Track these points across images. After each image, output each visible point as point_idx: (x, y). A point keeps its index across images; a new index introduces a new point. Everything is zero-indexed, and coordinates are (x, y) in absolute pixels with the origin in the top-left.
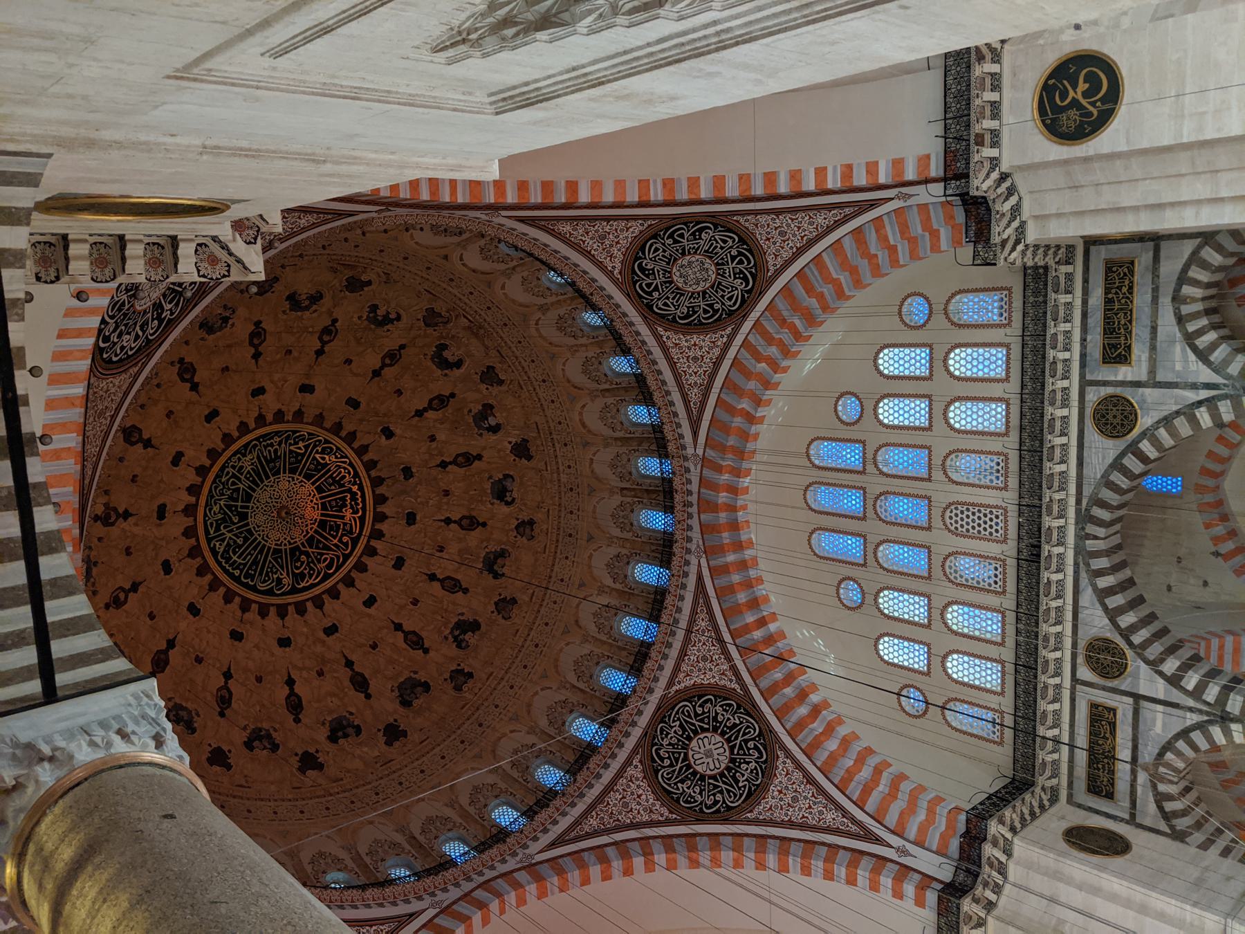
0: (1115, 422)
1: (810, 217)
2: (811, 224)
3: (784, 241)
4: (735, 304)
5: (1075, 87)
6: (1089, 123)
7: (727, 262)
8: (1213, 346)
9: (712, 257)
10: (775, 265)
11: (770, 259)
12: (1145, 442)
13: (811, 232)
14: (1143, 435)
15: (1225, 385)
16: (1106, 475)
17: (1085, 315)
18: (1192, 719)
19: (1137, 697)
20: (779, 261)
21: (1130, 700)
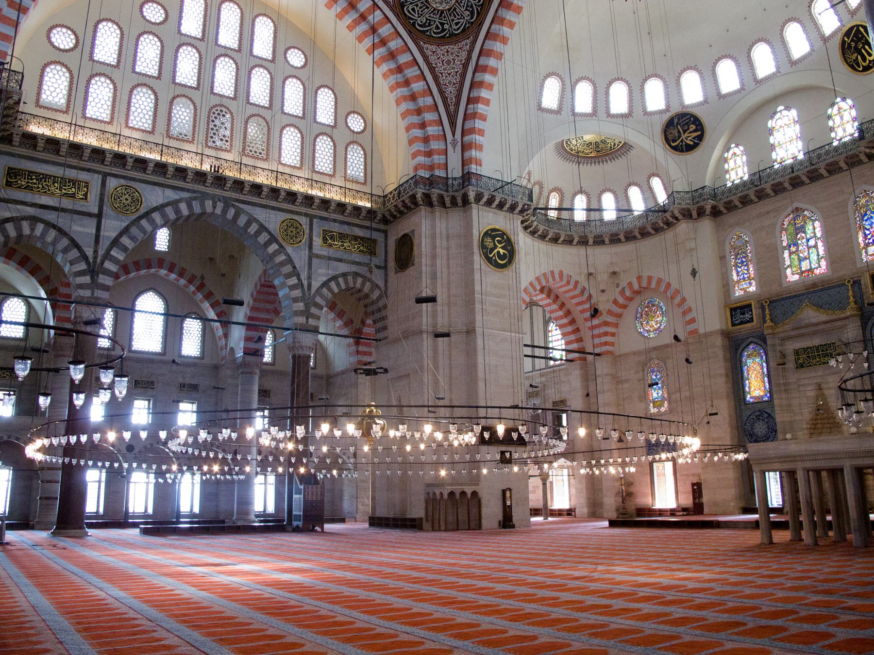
0: (294, 234)
1: (454, 84)
2: (450, 82)
3: (443, 61)
4: (409, 12)
5: (502, 248)
6: (487, 252)
7: (441, 19)
8: (330, 289)
9: (449, 11)
10: (427, 49)
11: (433, 48)
12: (277, 247)
13: (444, 80)
14: (281, 246)
15: (310, 294)
16: (257, 221)
17: (349, 224)
18: (89, 252)
19: (99, 216)
20: (429, 53)
21: (95, 210)
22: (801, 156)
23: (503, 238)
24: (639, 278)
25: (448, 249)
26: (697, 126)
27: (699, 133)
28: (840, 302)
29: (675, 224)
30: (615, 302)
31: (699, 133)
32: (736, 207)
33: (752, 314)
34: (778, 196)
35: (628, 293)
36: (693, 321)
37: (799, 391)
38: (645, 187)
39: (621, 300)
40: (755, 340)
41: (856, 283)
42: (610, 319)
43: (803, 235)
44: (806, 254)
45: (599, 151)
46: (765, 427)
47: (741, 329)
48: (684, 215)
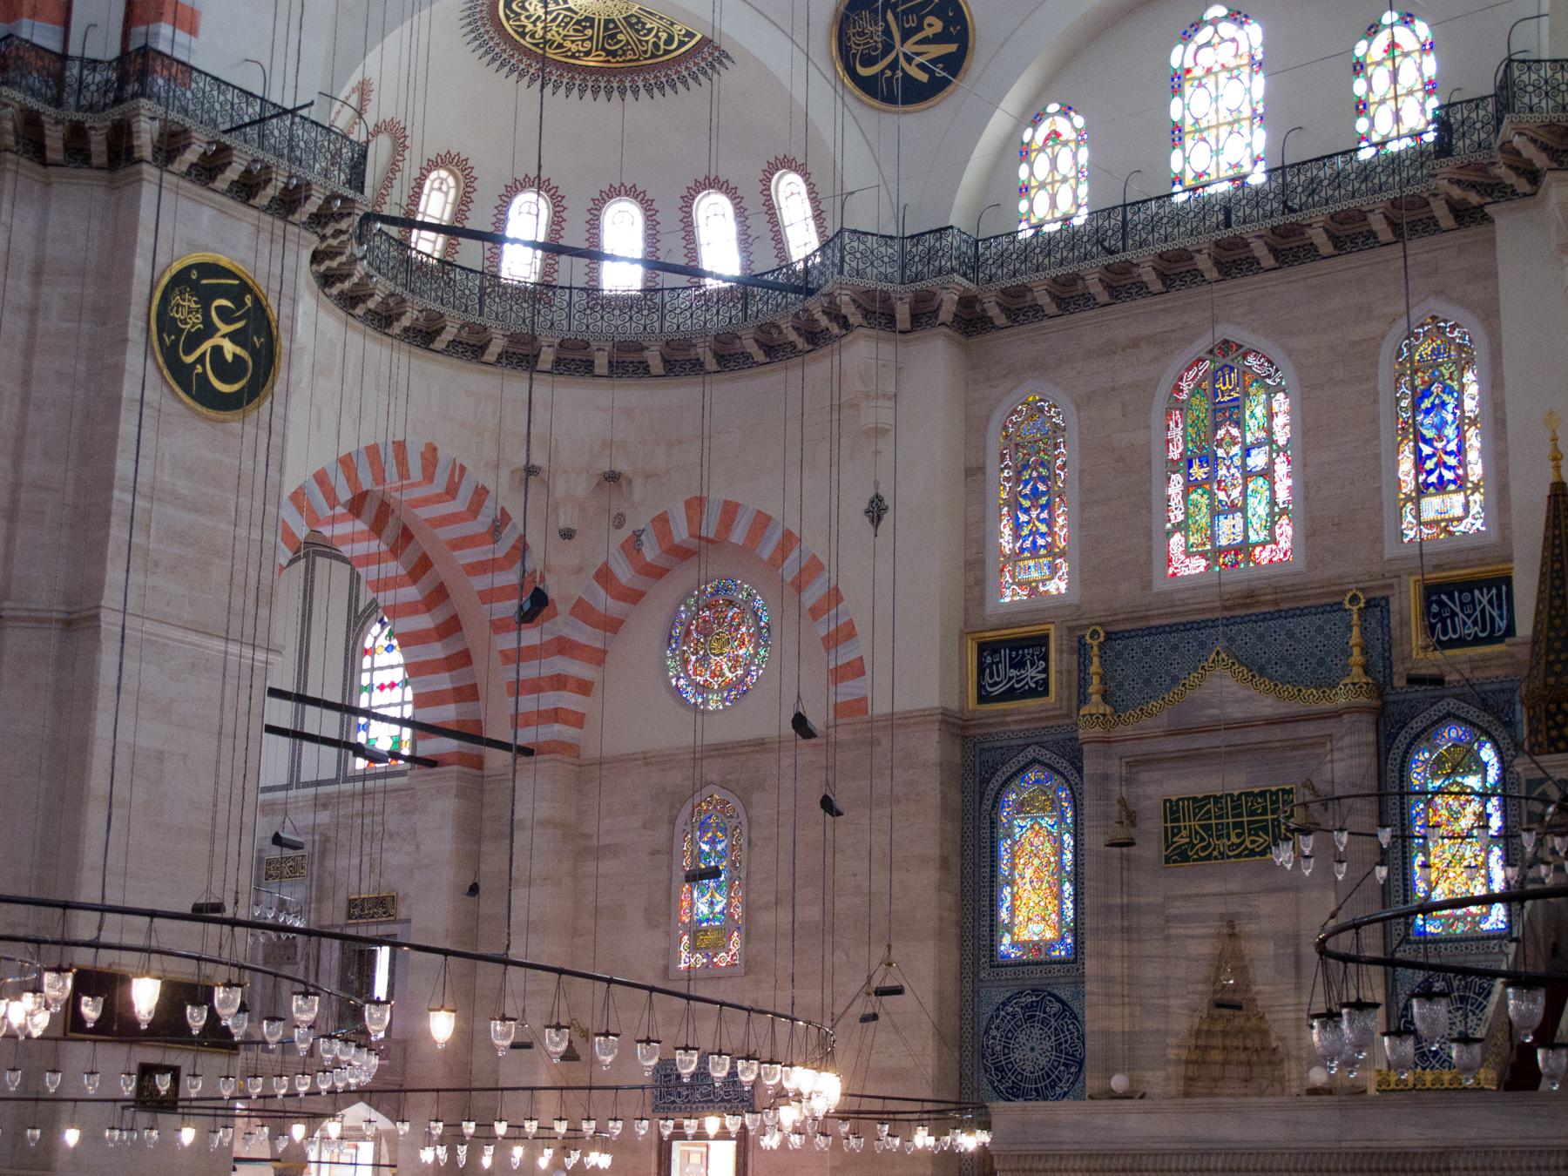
5: (232, 337)
22: (1258, 178)
23: (240, 303)
24: (696, 506)
25: (33, 312)
26: (947, 23)
27: (952, 48)
28: (1321, 663)
29: (832, 339)
30: (604, 576)
31: (952, 48)
32: (1037, 312)
33: (1046, 670)
34: (1173, 294)
35: (650, 551)
36: (856, 669)
37: (1167, 938)
38: (753, 202)
39: (625, 574)
40: (1047, 756)
41: (1376, 606)
42: (584, 634)
43: (1235, 432)
44: (1235, 493)
45: (613, 54)
46: (1047, 1044)
47: (1005, 713)
48: (867, 314)
